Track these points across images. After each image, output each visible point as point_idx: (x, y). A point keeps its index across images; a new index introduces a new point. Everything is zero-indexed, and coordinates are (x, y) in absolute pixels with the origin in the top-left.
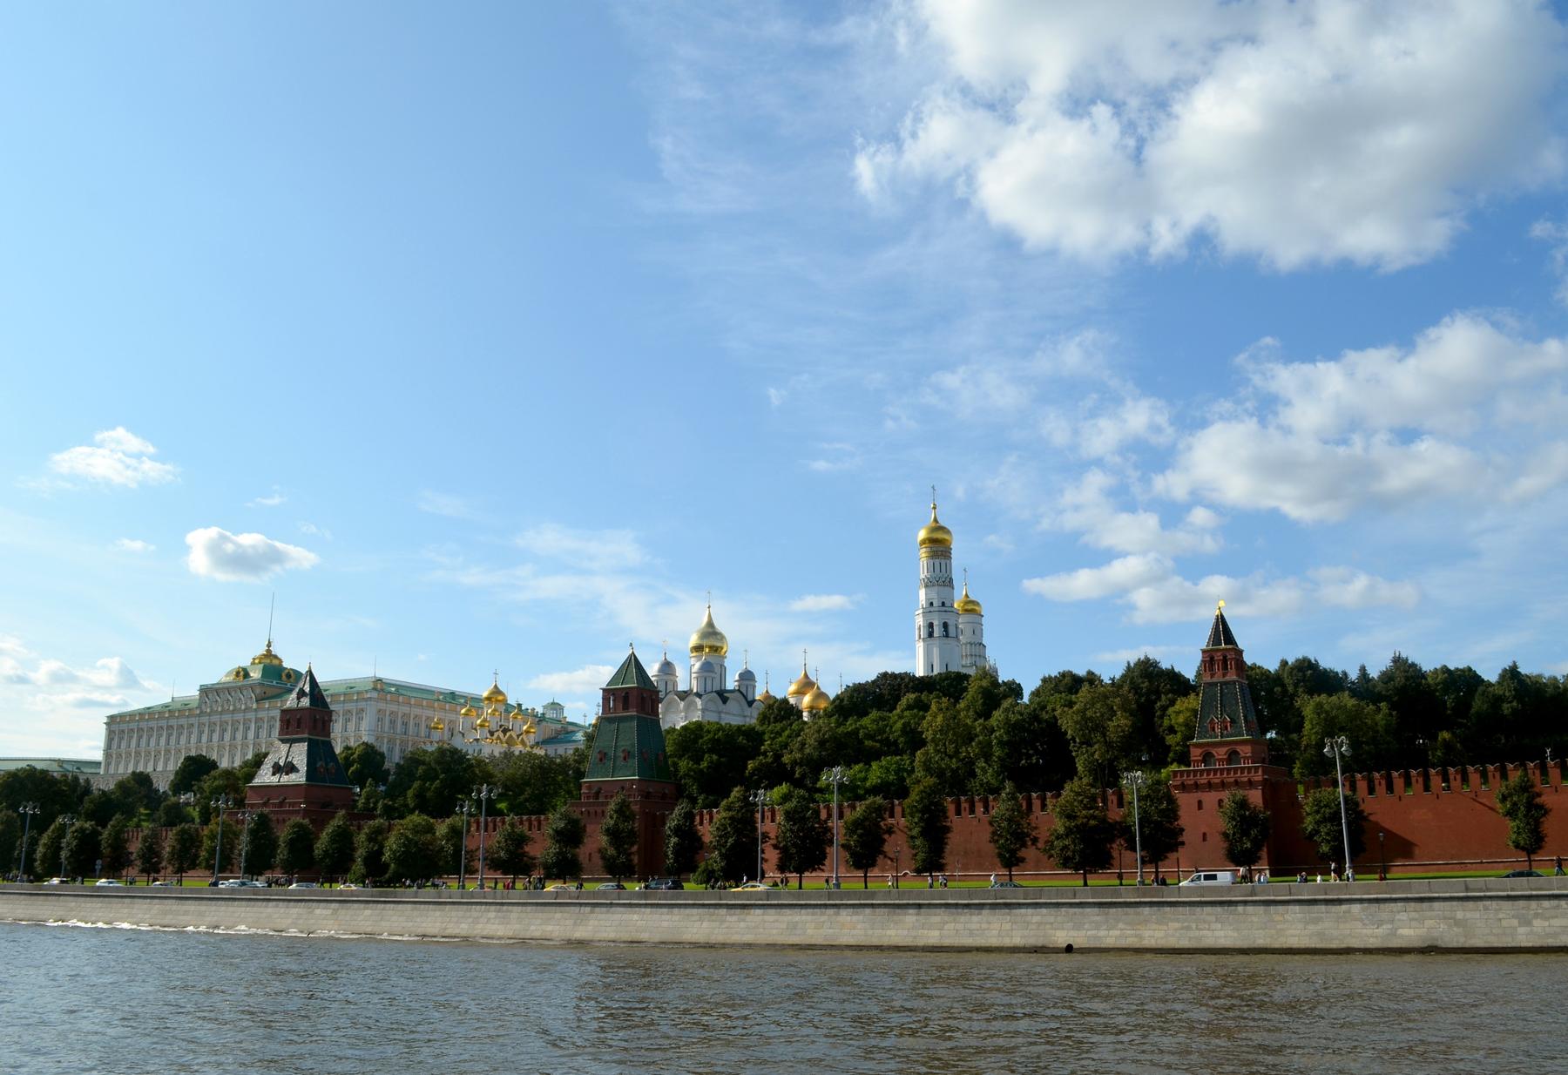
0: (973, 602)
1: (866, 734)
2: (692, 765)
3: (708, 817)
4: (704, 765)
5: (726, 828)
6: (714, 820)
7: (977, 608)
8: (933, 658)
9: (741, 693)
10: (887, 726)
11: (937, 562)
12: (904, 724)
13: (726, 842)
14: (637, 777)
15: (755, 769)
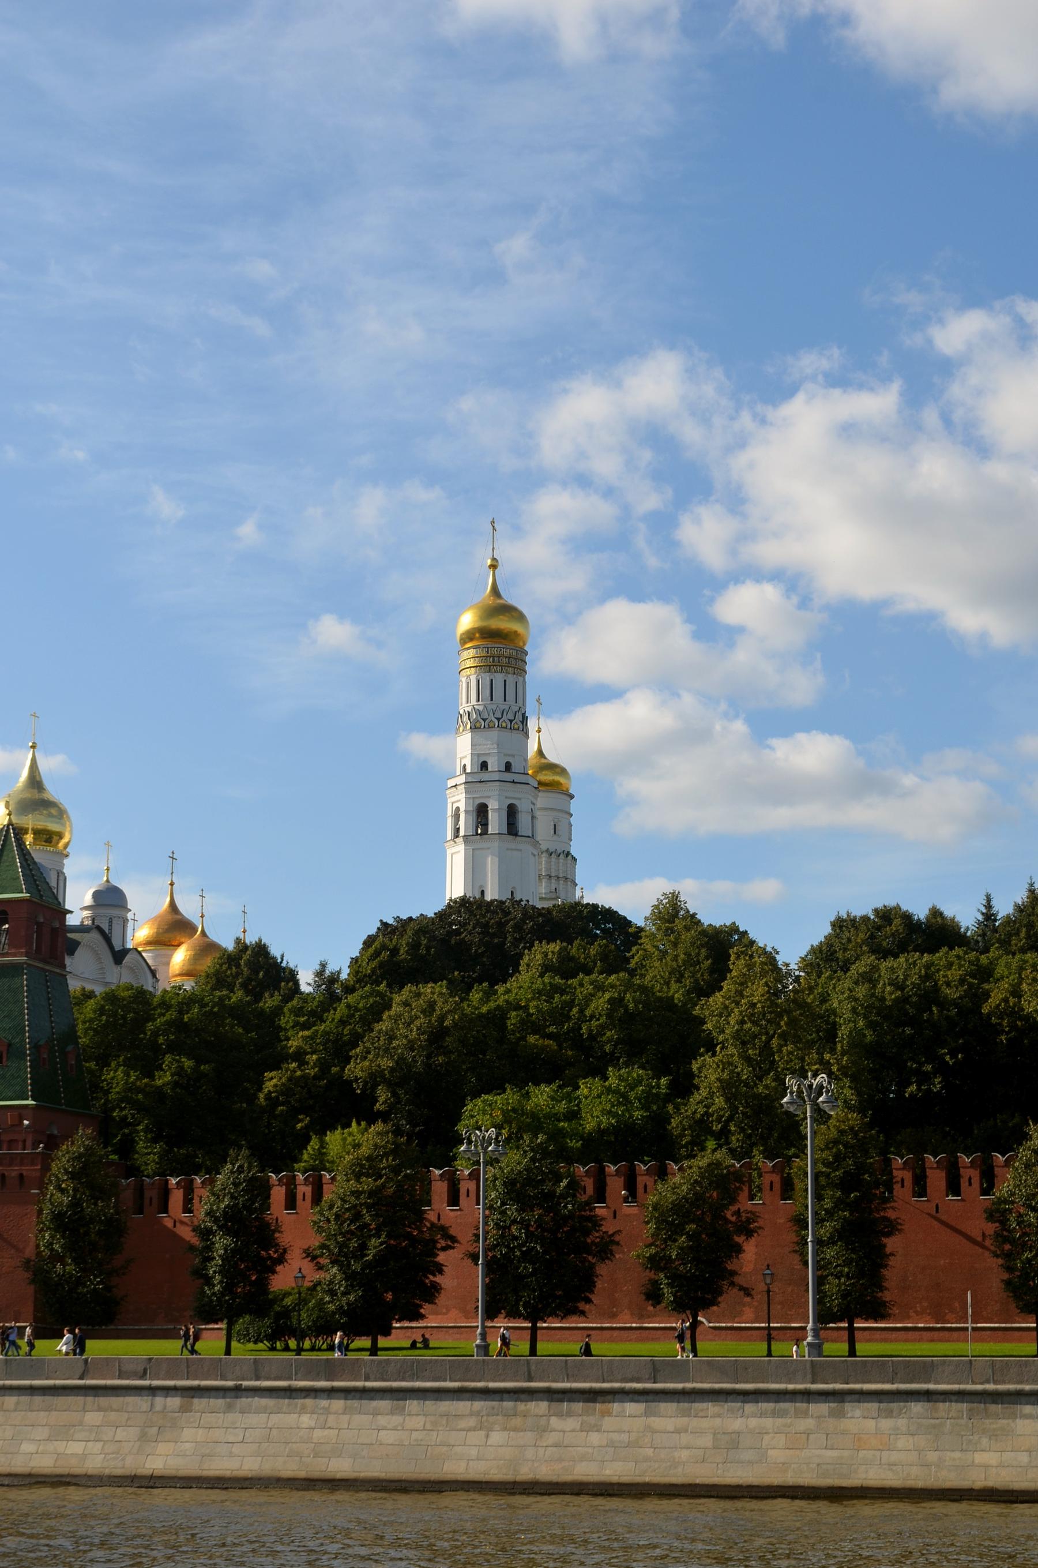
0: (552, 767)
1: (522, 1022)
2: (138, 1078)
3: (308, 1190)
4: (164, 1079)
5: (357, 1216)
6: (327, 1197)
7: (562, 780)
8: (485, 875)
9: (99, 929)
10: (571, 1004)
11: (499, 678)
12: (611, 1001)
13: (363, 1247)
14: (30, 1102)
15: (286, 1091)
